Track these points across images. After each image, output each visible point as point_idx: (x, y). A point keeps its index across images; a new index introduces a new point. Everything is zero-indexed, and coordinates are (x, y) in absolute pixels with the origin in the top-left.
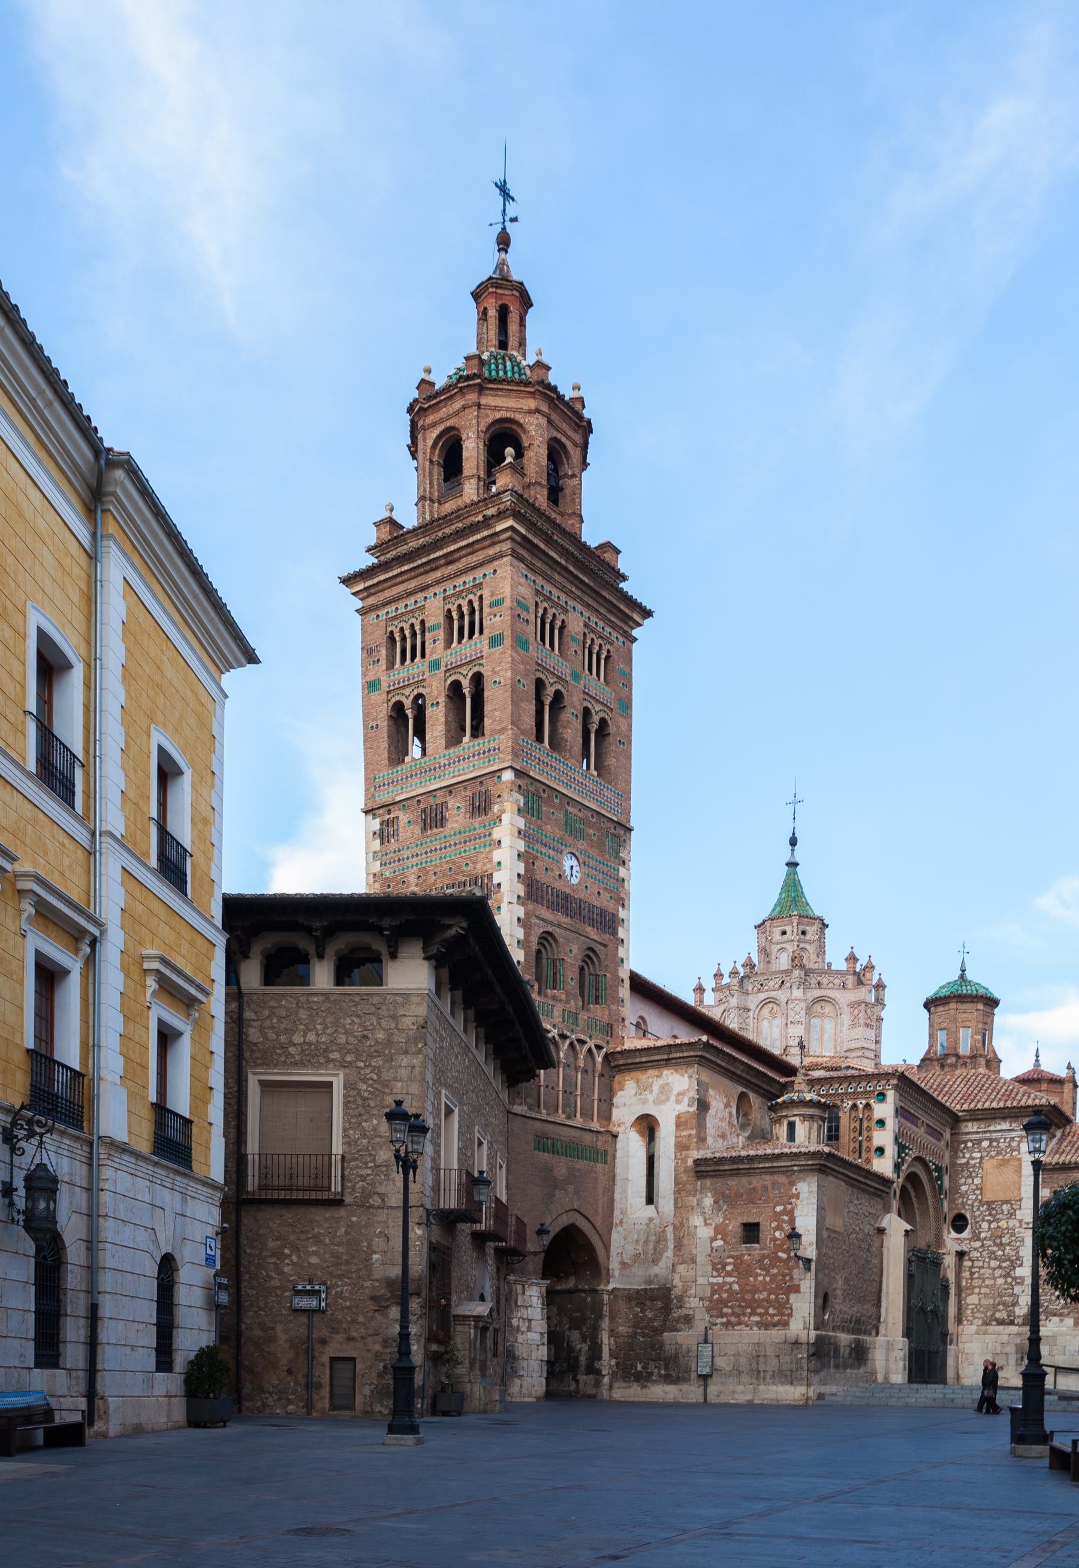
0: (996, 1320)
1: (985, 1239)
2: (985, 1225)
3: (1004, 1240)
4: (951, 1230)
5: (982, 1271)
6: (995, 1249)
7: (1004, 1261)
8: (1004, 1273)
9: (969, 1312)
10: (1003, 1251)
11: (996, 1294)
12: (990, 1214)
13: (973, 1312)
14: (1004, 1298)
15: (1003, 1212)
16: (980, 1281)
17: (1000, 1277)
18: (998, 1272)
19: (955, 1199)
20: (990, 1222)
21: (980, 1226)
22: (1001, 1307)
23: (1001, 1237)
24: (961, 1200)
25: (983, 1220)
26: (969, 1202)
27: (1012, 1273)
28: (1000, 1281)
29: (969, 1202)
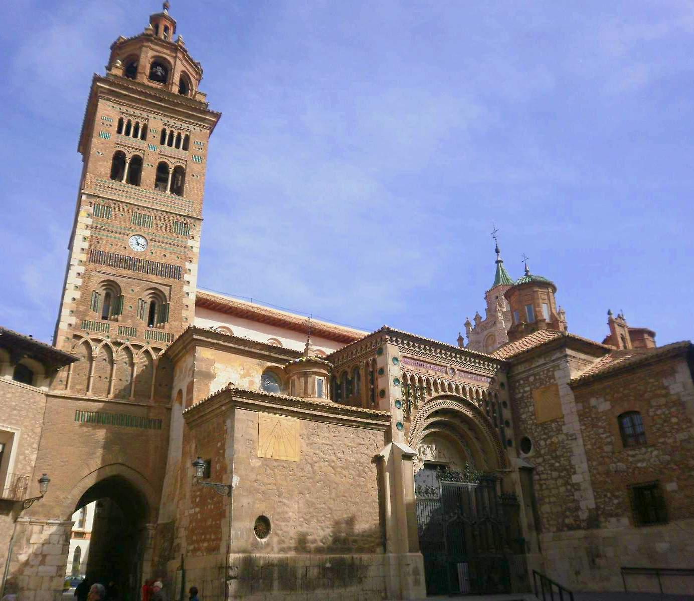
1: (545, 454)
3: (558, 453)
4: (521, 452)
5: (548, 482)
6: (553, 461)
7: (562, 472)
8: (563, 482)
10: (559, 462)
12: (545, 434)
15: (553, 430)
17: (561, 486)
18: (560, 482)
23: (555, 451)
25: (541, 439)
26: (529, 427)
27: (569, 480)
28: (562, 489)
29: (529, 427)
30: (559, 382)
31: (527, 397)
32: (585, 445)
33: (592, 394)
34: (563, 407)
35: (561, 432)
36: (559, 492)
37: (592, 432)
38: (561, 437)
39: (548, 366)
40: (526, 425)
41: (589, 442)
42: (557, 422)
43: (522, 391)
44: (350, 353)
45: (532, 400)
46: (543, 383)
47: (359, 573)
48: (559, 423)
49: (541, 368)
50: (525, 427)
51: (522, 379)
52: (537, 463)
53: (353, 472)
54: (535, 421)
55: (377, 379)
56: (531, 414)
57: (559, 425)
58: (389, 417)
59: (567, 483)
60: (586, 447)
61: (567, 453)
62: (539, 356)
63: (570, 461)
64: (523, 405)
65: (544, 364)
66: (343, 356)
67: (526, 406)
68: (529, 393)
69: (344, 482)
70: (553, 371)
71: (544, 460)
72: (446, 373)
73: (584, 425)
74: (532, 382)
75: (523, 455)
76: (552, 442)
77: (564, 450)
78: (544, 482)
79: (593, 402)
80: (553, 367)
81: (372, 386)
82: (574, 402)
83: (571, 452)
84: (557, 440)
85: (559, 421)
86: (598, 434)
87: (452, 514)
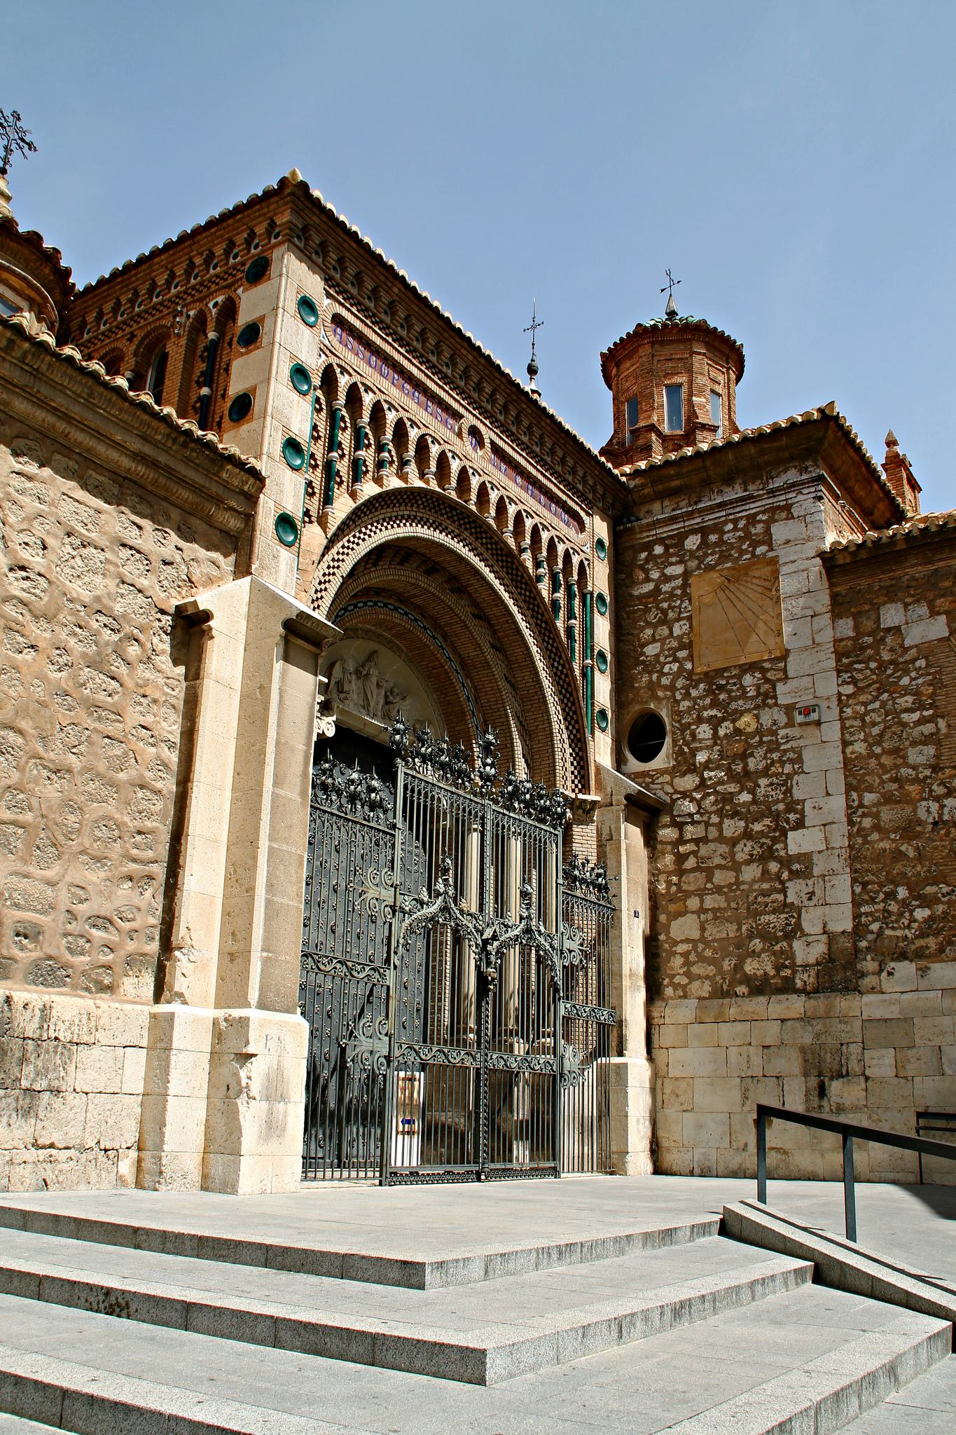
0: (747, 980)
1: (707, 765)
2: (704, 731)
5: (704, 850)
6: (732, 788)
7: (756, 820)
9: (677, 962)
10: (752, 792)
11: (743, 911)
12: (714, 704)
13: (687, 963)
14: (765, 918)
15: (744, 695)
16: (701, 877)
17: (748, 863)
18: (744, 851)
19: (634, 679)
20: (715, 723)
21: (693, 735)
22: (757, 944)
23: (744, 757)
24: (645, 678)
25: (700, 720)
28: (751, 872)
29: (665, 681)
30: (784, 554)
31: (671, 595)
32: (845, 744)
33: (891, 594)
34: (787, 629)
35: (770, 701)
36: (738, 883)
37: (877, 705)
38: (767, 718)
39: (753, 507)
40: (655, 677)
41: (862, 736)
42: (764, 671)
43: (655, 575)
44: (147, 285)
45: (686, 603)
46: (730, 555)
47: (29, 1070)
48: (769, 675)
49: (731, 511)
50: (651, 681)
51: (661, 541)
52: (676, 792)
53: (72, 642)
54: (689, 666)
55: (227, 370)
56: (675, 644)
57: (767, 681)
58: (255, 474)
59: (767, 855)
60: (849, 749)
61: (782, 763)
62: (728, 481)
63: (789, 791)
64: (652, 617)
65: (742, 499)
66: (118, 300)
67: (664, 621)
68: (679, 582)
69: (24, 670)
70: (768, 524)
71: (703, 780)
72: (459, 435)
73: (854, 681)
74: (690, 551)
75: (634, 764)
76: (738, 731)
77: (775, 756)
78: (689, 847)
79: (892, 615)
80: (773, 510)
81: (205, 391)
82: (829, 615)
83: (800, 760)
84: (754, 726)
85: (768, 670)
86: (897, 714)
87: (425, 896)
